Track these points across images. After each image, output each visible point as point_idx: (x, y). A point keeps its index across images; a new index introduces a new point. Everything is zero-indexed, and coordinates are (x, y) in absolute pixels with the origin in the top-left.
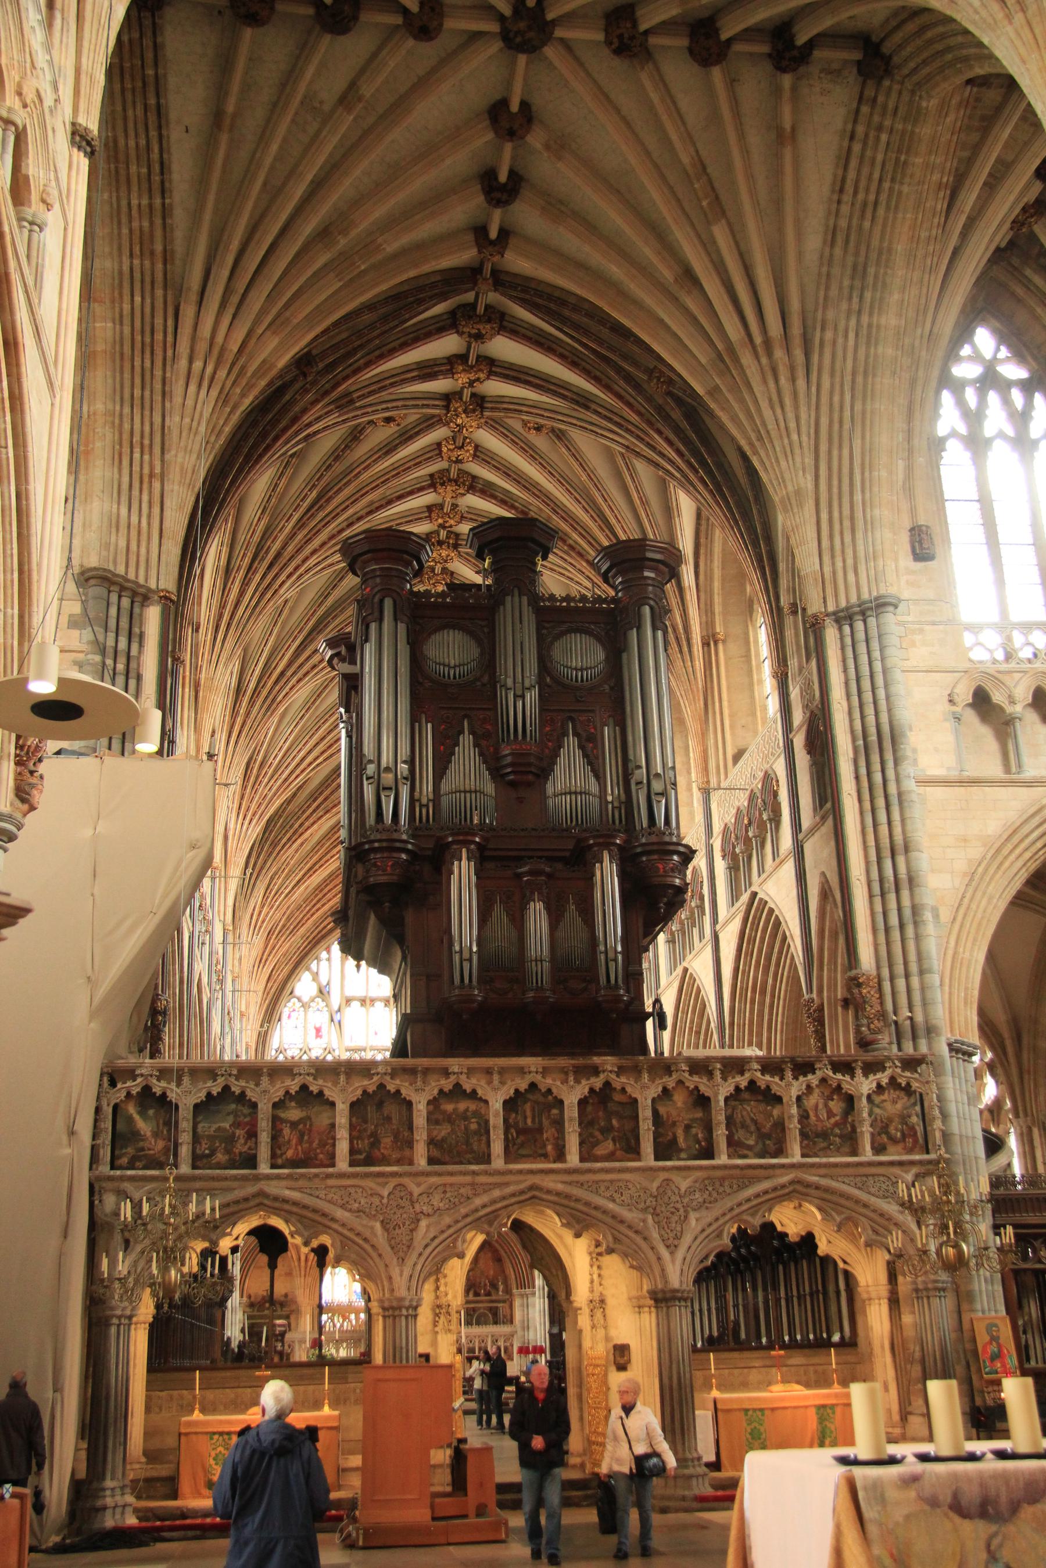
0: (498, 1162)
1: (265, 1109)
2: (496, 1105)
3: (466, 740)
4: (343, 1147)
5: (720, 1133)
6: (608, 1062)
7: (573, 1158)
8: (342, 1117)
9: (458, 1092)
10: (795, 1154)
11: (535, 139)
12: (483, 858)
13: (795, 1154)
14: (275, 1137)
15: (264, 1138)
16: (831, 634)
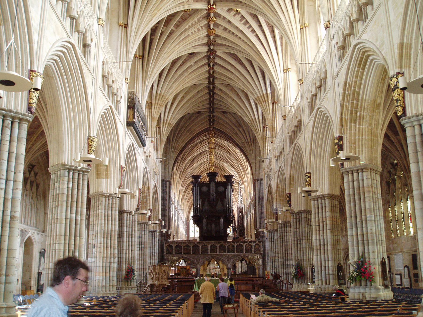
0: (209, 253)
1: (183, 247)
2: (209, 246)
3: (206, 201)
4: (191, 251)
5: (235, 250)
6: (222, 242)
7: (218, 253)
8: (191, 247)
9: (205, 245)
10: (244, 252)
11: (215, 118)
12: (207, 219)
13: (244, 252)
14: (184, 250)
15: (183, 250)
16: (256, 182)
